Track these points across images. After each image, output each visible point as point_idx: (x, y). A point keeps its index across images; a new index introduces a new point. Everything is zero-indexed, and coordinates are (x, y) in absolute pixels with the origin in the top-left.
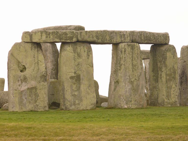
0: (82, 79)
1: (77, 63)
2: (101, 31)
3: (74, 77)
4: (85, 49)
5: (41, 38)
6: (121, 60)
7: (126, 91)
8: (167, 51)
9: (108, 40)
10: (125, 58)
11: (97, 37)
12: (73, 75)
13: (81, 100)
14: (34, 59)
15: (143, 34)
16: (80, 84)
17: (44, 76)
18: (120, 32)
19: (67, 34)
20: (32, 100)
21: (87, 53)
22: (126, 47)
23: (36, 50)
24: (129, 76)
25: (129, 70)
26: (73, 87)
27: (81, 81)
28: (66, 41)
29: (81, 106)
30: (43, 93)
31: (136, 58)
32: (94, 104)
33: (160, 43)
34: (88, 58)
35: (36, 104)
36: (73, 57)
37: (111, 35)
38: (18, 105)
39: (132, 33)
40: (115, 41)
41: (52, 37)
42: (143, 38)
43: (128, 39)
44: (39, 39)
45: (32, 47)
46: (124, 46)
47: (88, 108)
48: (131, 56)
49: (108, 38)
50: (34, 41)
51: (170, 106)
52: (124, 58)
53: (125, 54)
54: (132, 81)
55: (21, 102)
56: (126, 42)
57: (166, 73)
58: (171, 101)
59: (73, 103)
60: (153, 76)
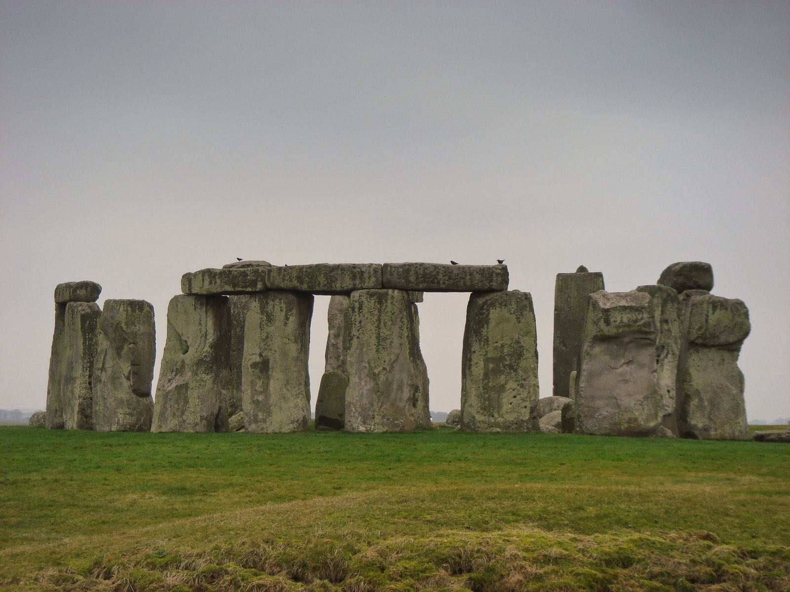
0: (273, 368)
1: (266, 335)
2: (310, 267)
4: (283, 305)
7: (362, 395)
8: (493, 305)
9: (322, 284)
10: (360, 322)
11: (299, 279)
13: (269, 413)
14: (199, 327)
15: (413, 269)
16: (268, 378)
17: (206, 361)
18: (354, 266)
20: (178, 409)
21: (286, 312)
22: (363, 299)
23: (204, 309)
24: (368, 361)
25: (369, 348)
27: (270, 373)
28: (244, 289)
29: (268, 424)
34: (286, 324)
37: (332, 274)
39: (385, 269)
40: (338, 285)
41: (218, 281)
42: (412, 278)
43: (372, 282)
46: (360, 296)
47: (283, 430)
48: (376, 317)
49: (322, 279)
50: (194, 291)
51: (498, 430)
53: (361, 314)
54: (374, 374)
55: (162, 414)
57: (485, 355)
58: (500, 420)
59: (252, 418)
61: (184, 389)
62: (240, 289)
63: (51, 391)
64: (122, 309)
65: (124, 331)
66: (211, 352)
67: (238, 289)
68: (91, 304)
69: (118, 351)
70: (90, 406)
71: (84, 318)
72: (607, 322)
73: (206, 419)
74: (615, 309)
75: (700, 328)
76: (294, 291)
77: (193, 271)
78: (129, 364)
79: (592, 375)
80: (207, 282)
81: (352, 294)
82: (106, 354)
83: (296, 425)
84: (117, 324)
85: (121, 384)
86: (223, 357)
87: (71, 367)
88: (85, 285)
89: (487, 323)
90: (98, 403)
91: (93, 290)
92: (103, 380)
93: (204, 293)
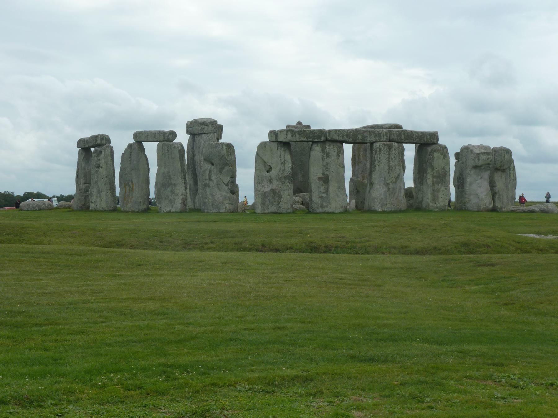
4: (336, 149)
6: (375, 161)
7: (381, 194)
8: (435, 151)
11: (347, 135)
12: (321, 176)
16: (328, 186)
22: (381, 147)
23: (283, 149)
30: (287, 194)
31: (394, 159)
33: (427, 143)
34: (338, 158)
41: (298, 136)
42: (403, 137)
49: (360, 137)
50: (279, 140)
54: (388, 184)
58: (438, 205)
60: (419, 178)
67: (309, 140)
69: (221, 171)
72: (479, 160)
74: (481, 153)
75: (501, 162)
79: (471, 184)
80: (290, 135)
82: (210, 171)
89: (433, 159)
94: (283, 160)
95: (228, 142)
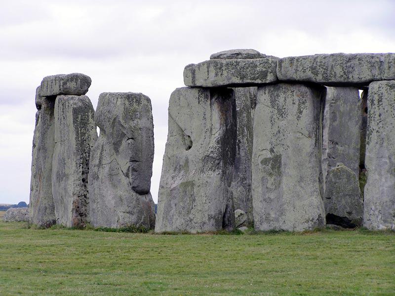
1: (277, 130)
3: (270, 159)
4: (296, 98)
5: (208, 78)
10: (380, 115)
11: (313, 69)
12: (269, 155)
13: (282, 213)
14: (204, 121)
16: (280, 174)
17: (212, 157)
18: (372, 56)
19: (256, 66)
20: (183, 208)
22: (383, 91)
26: (267, 182)
27: (282, 169)
28: (253, 81)
32: (312, 221)
35: (190, 218)
36: (270, 115)
37: (349, 64)
38: (162, 219)
40: (356, 76)
44: (206, 80)
45: (199, 96)
49: (338, 71)
50: (198, 84)
52: (377, 116)
56: (385, 80)
59: (264, 217)
61: (190, 187)
62: (250, 81)
63: (35, 188)
64: (119, 103)
65: (122, 126)
66: (217, 148)
68: (82, 97)
69: (116, 146)
70: (86, 204)
71: (76, 111)
73: (214, 218)
76: (308, 83)
77: (196, 62)
78: (128, 161)
80: (212, 74)
81: (371, 86)
83: (310, 224)
84: (115, 119)
85: (120, 181)
86: (229, 152)
87: (63, 162)
88: (74, 77)
90: (96, 201)
91: (85, 82)
92: (100, 177)
93: (210, 85)
94: (208, 126)
95: (135, 90)
